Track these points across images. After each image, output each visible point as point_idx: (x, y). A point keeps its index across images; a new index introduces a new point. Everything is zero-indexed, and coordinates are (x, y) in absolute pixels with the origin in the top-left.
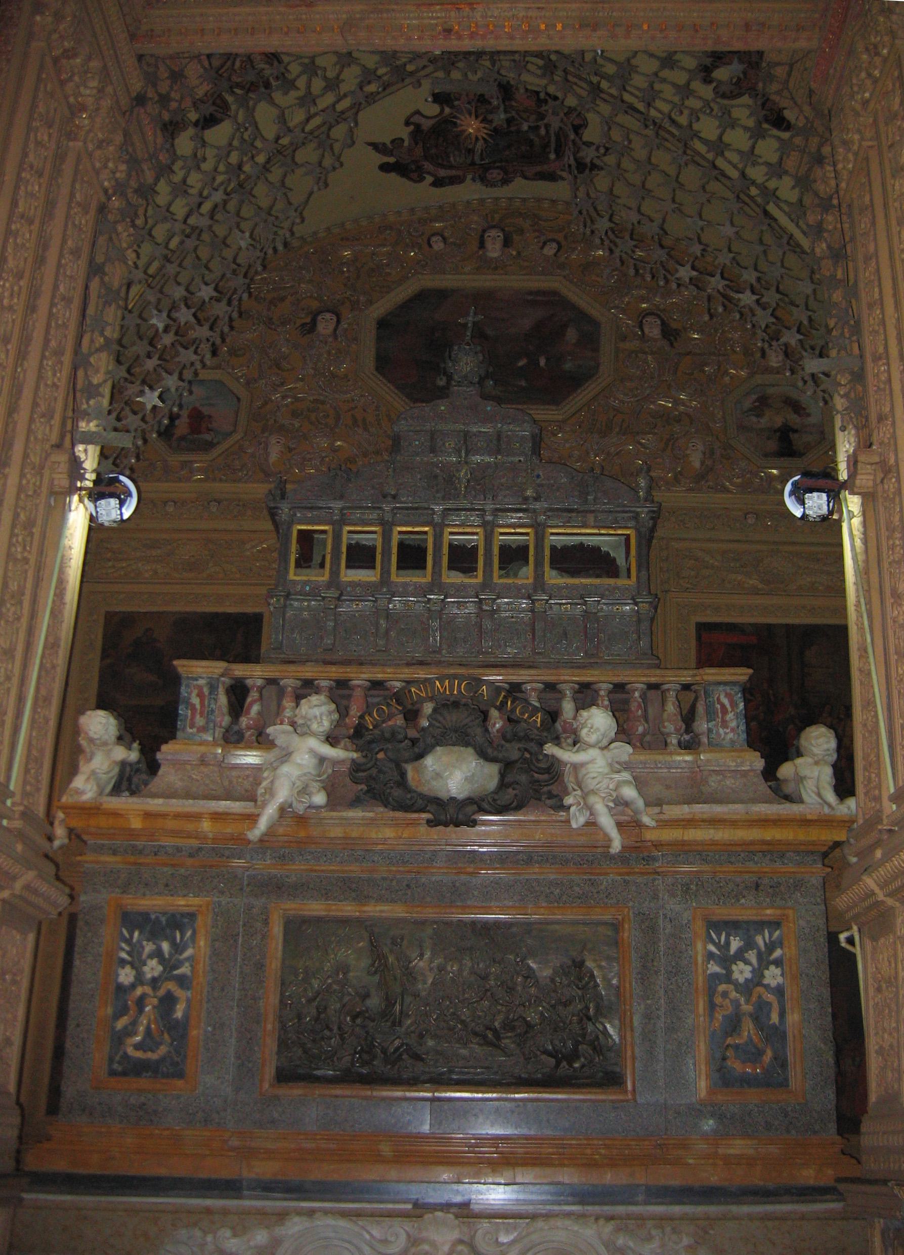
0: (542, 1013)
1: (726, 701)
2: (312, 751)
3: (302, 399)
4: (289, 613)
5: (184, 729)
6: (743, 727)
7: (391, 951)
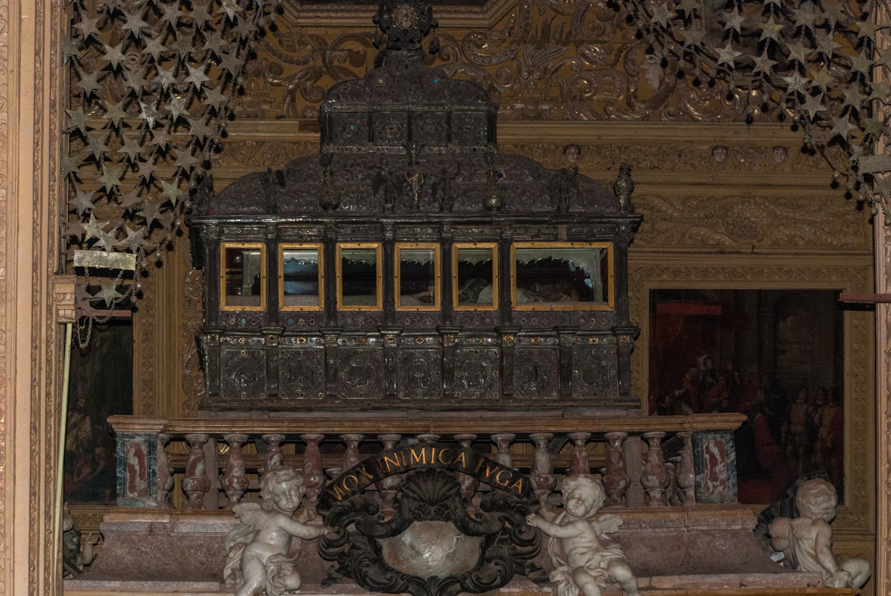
1: (715, 451)
2: (281, 529)
4: (225, 351)
5: (124, 495)
6: (733, 480)
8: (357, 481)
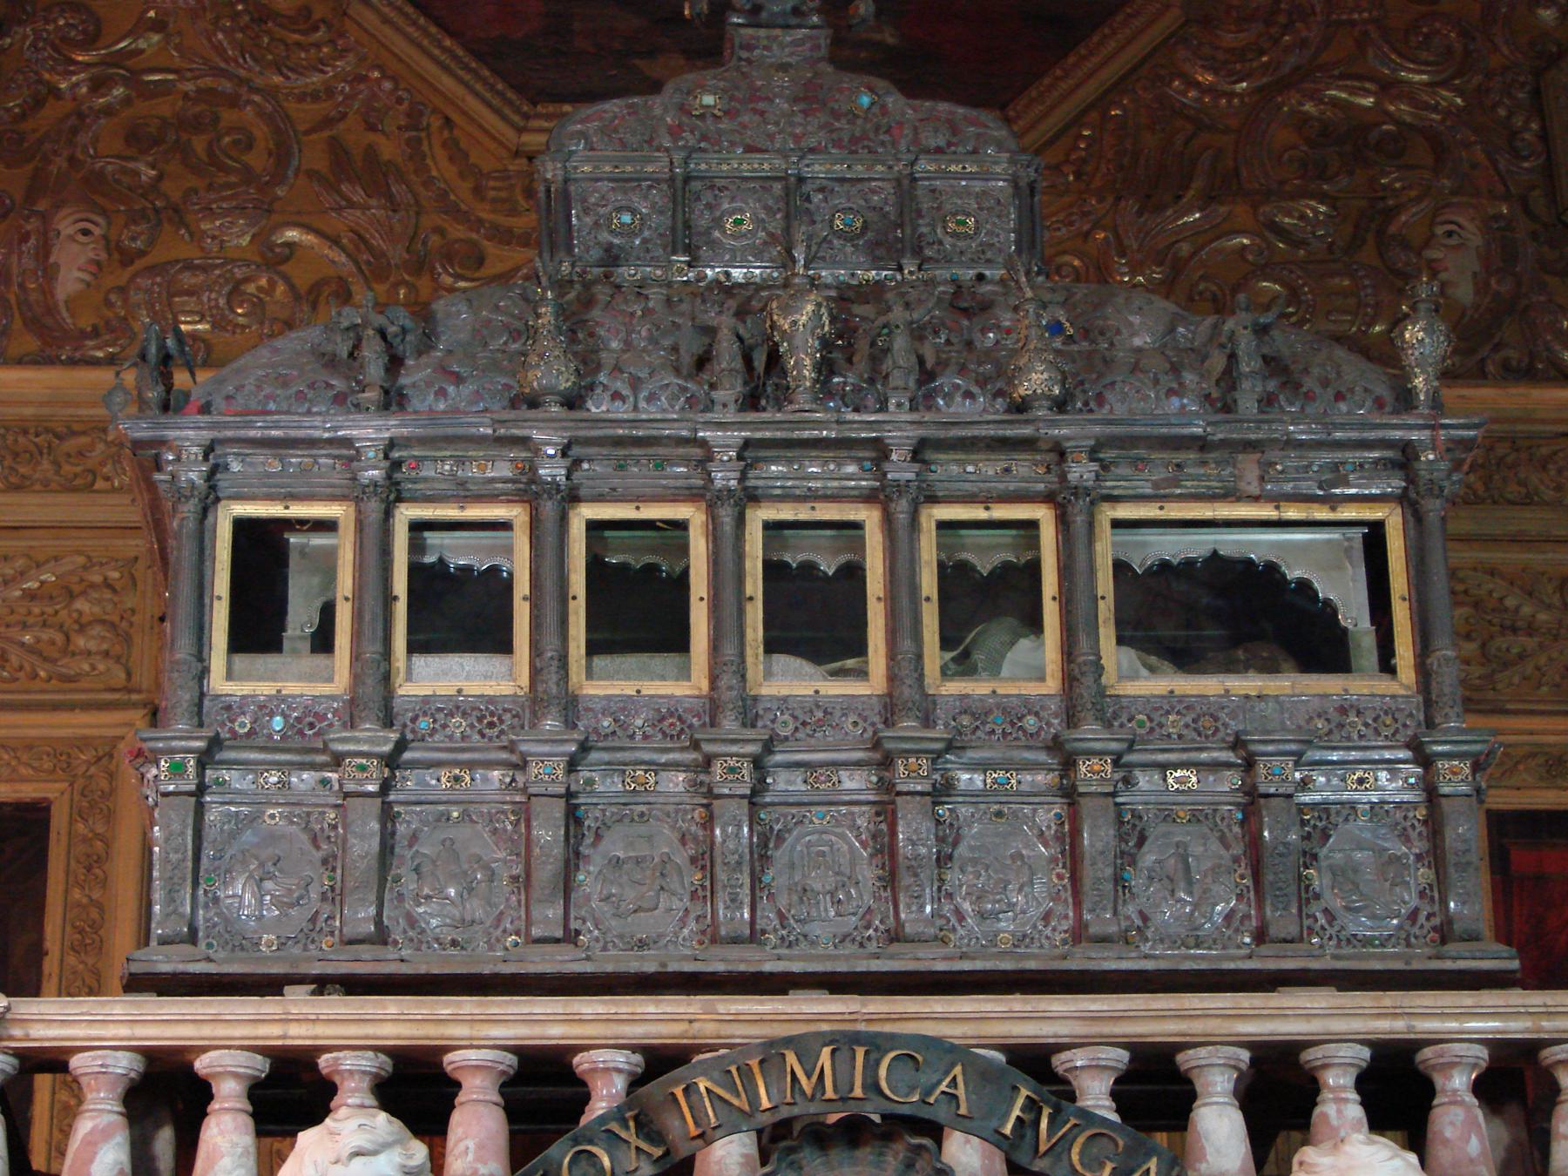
3: (162, 89)
8: (606, 1162)
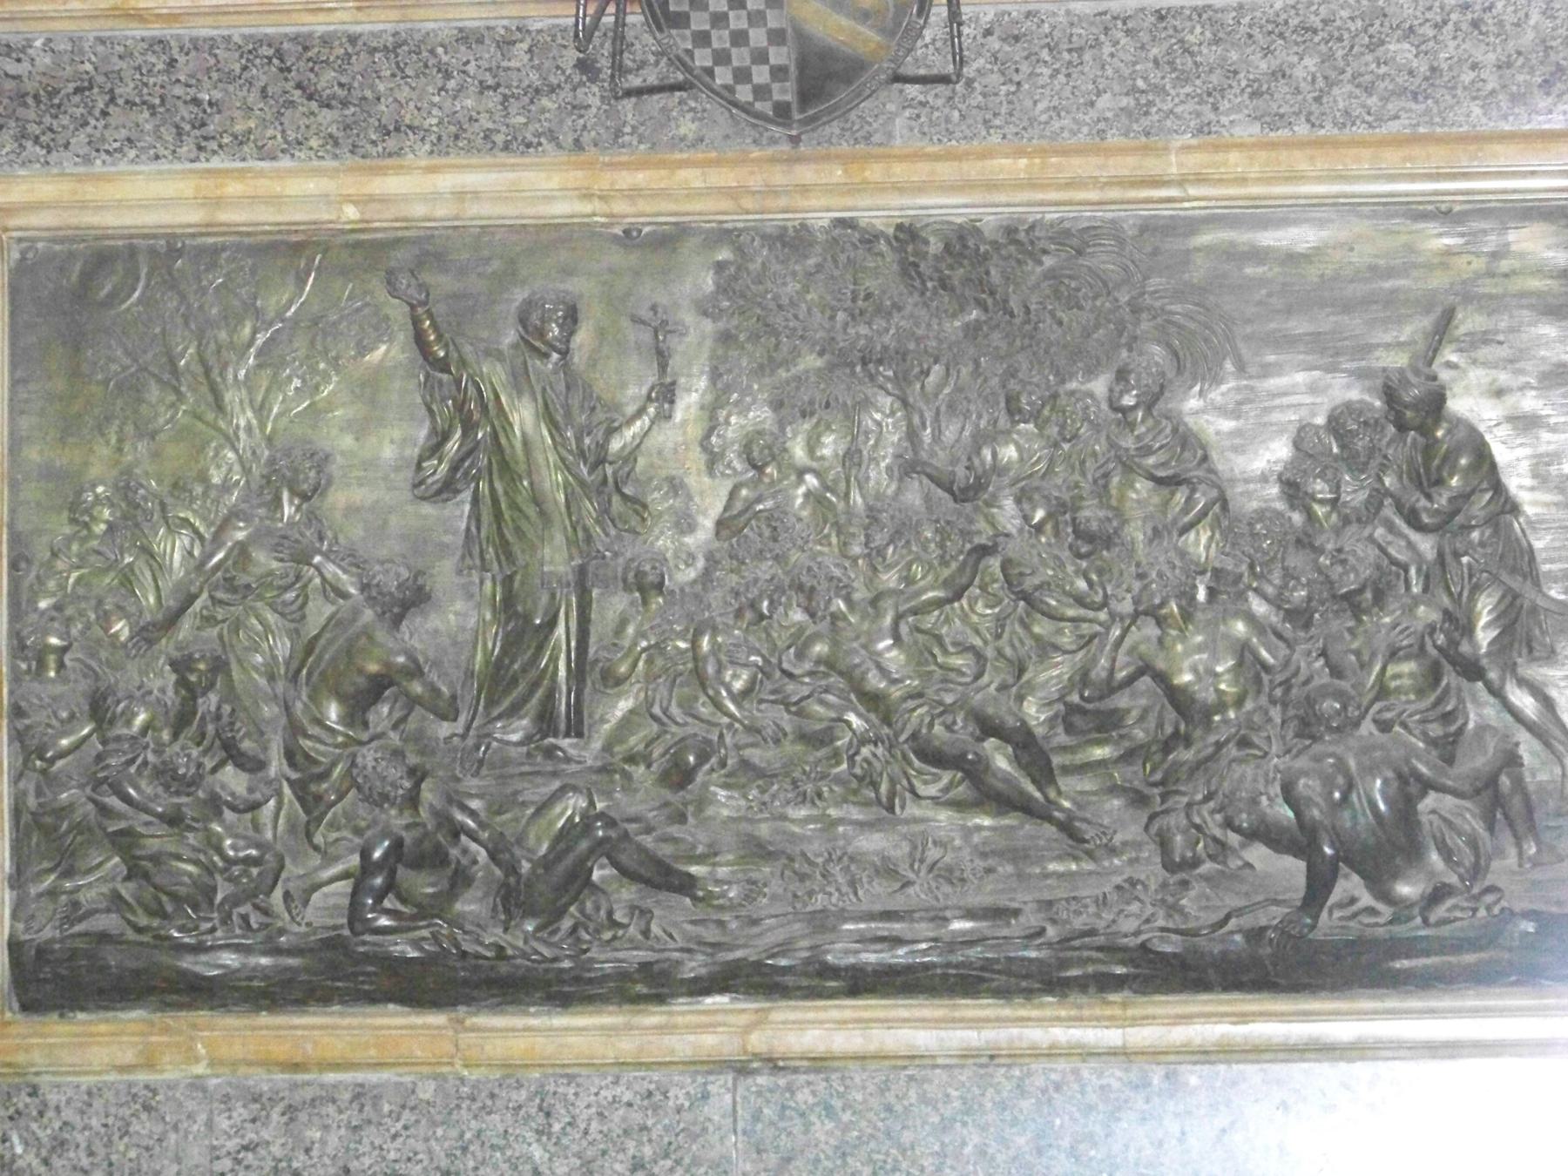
0: (1243, 652)
7: (520, 380)
